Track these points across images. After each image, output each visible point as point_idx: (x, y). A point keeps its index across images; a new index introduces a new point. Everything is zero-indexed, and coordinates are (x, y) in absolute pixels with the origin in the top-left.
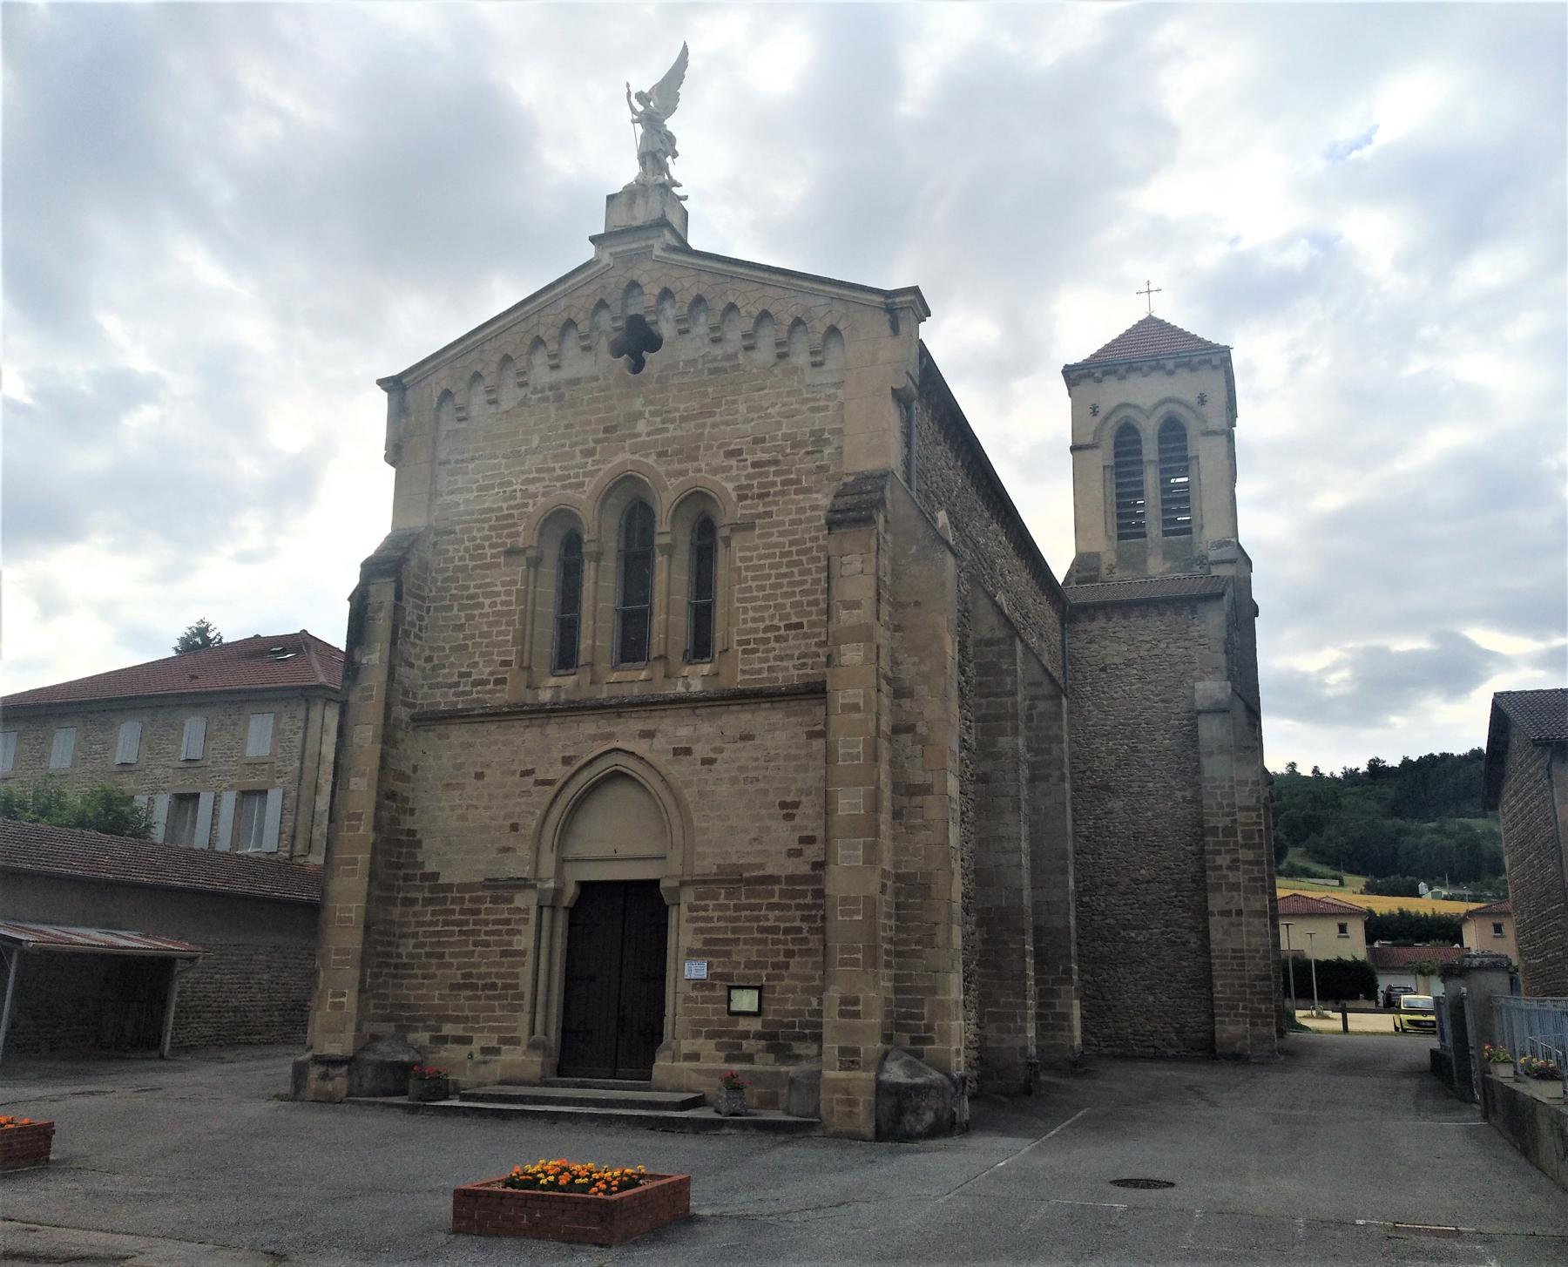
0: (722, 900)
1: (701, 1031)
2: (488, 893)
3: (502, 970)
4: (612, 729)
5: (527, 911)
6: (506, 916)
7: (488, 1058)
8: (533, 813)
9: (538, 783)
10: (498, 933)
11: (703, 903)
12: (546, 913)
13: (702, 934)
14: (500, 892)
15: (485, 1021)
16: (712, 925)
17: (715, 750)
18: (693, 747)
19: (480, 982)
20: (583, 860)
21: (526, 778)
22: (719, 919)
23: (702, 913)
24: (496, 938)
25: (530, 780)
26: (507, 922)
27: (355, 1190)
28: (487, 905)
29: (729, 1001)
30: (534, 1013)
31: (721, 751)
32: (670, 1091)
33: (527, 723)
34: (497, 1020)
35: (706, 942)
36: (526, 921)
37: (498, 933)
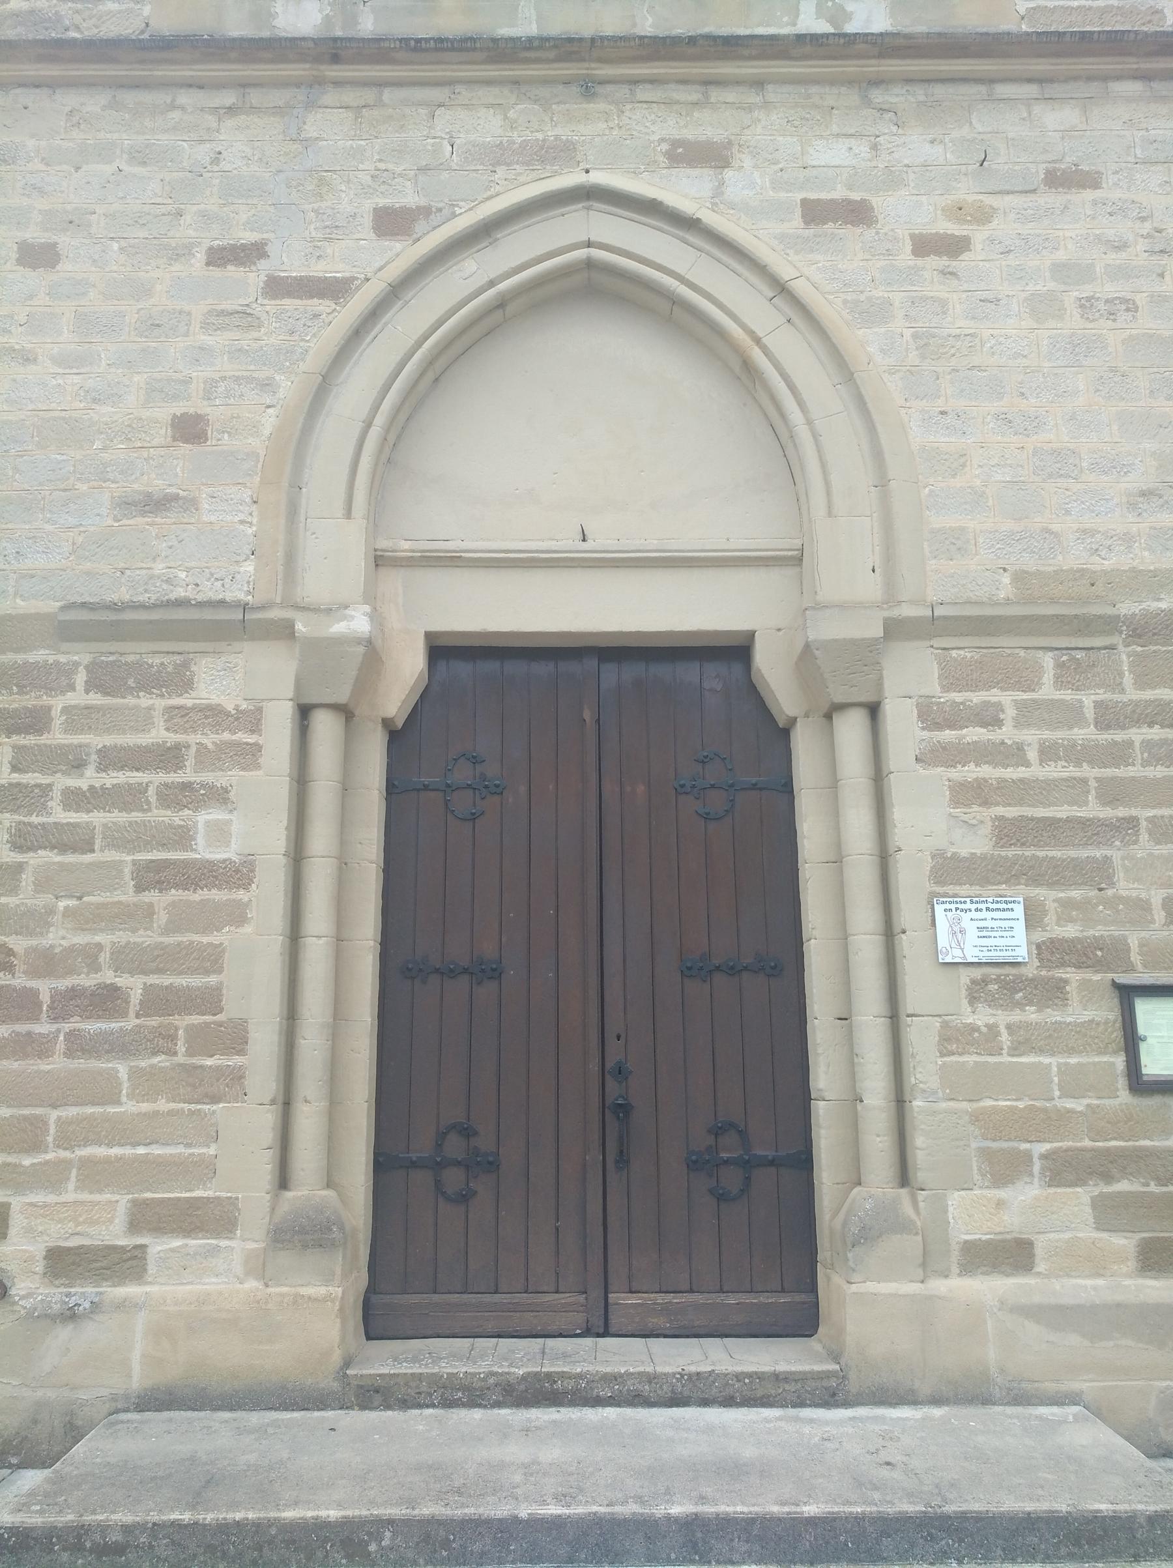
0: (1047, 690)
1: (1027, 1157)
2: (80, 655)
3: (146, 938)
4: (564, 132)
5: (252, 719)
6: (159, 734)
7: (83, 1293)
8: (267, 385)
9: (277, 287)
10: (130, 798)
11: (976, 698)
12: (325, 726)
13: (986, 803)
14: (134, 652)
15: (66, 1140)
16: (1021, 772)
17: (958, 211)
18: (875, 201)
19: (45, 988)
20: (453, 561)
21: (233, 271)
22: (1048, 753)
23: (974, 734)
24: (118, 817)
25: (254, 278)
26: (169, 757)
27: (572, 1542)
28: (78, 697)
29: (1131, 1042)
30: (286, 1104)
31: (983, 216)
32: (936, 1400)
33: (228, 98)
34: (120, 1132)
35: (1007, 832)
36: (249, 756)
37: (130, 798)
